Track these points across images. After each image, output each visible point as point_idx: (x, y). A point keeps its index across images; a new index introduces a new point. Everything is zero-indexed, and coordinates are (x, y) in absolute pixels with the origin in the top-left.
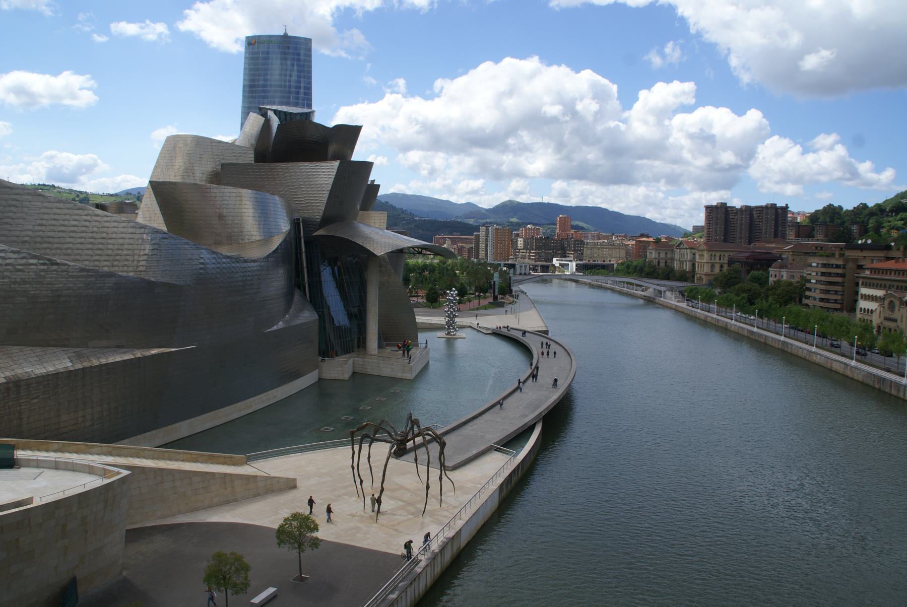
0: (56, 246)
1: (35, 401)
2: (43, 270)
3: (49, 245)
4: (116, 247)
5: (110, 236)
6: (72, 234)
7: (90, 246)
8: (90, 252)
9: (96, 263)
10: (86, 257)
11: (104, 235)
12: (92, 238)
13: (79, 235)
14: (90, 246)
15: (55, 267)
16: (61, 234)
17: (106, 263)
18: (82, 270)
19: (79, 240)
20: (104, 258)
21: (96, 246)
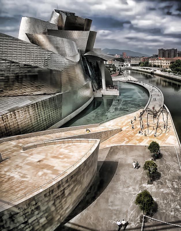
0: (9, 55)
1: (23, 117)
2: (9, 65)
3: (6, 55)
4: (35, 56)
5: (31, 52)
6: (15, 51)
7: (24, 56)
8: (24, 58)
9: (28, 63)
10: (24, 60)
11: (29, 51)
12: (24, 52)
13: (18, 51)
14: (24, 56)
15: (14, 64)
16: (10, 50)
17: (32, 63)
18: (25, 65)
19: (19, 53)
20: (31, 61)
21: (27, 56)
